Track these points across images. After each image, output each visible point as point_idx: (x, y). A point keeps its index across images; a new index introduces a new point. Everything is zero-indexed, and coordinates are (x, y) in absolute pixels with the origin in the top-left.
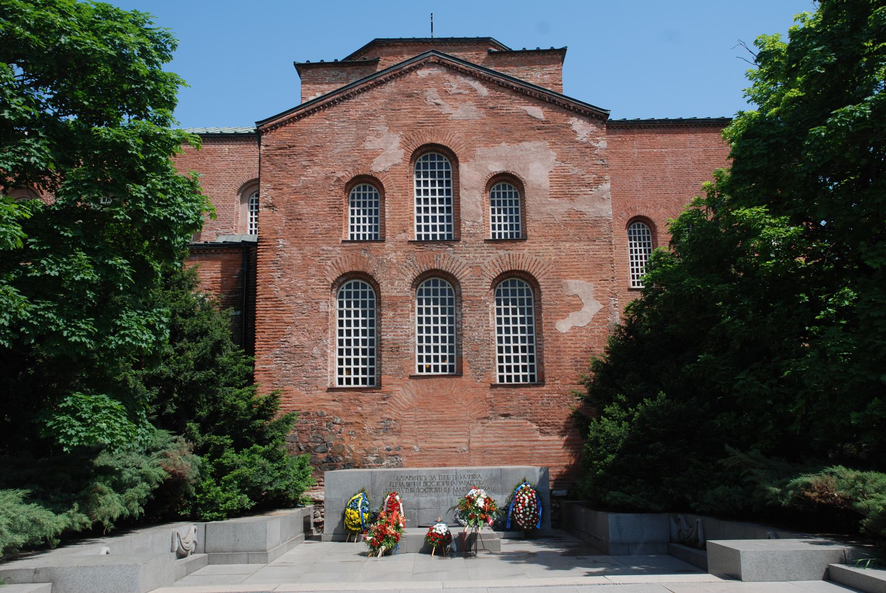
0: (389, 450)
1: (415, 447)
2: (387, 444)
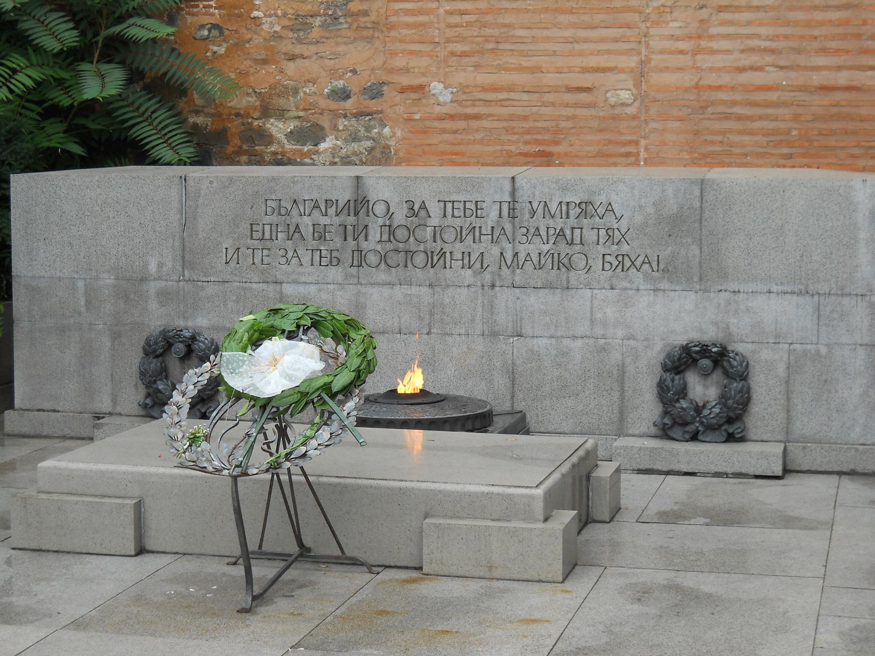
0: (344, 95)
1: (436, 87)
2: (334, 74)
